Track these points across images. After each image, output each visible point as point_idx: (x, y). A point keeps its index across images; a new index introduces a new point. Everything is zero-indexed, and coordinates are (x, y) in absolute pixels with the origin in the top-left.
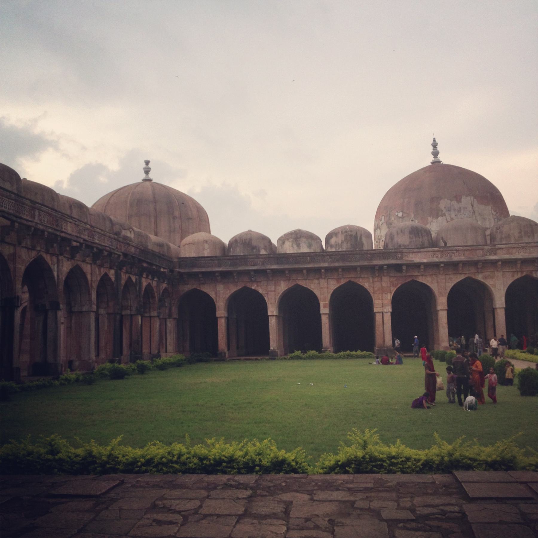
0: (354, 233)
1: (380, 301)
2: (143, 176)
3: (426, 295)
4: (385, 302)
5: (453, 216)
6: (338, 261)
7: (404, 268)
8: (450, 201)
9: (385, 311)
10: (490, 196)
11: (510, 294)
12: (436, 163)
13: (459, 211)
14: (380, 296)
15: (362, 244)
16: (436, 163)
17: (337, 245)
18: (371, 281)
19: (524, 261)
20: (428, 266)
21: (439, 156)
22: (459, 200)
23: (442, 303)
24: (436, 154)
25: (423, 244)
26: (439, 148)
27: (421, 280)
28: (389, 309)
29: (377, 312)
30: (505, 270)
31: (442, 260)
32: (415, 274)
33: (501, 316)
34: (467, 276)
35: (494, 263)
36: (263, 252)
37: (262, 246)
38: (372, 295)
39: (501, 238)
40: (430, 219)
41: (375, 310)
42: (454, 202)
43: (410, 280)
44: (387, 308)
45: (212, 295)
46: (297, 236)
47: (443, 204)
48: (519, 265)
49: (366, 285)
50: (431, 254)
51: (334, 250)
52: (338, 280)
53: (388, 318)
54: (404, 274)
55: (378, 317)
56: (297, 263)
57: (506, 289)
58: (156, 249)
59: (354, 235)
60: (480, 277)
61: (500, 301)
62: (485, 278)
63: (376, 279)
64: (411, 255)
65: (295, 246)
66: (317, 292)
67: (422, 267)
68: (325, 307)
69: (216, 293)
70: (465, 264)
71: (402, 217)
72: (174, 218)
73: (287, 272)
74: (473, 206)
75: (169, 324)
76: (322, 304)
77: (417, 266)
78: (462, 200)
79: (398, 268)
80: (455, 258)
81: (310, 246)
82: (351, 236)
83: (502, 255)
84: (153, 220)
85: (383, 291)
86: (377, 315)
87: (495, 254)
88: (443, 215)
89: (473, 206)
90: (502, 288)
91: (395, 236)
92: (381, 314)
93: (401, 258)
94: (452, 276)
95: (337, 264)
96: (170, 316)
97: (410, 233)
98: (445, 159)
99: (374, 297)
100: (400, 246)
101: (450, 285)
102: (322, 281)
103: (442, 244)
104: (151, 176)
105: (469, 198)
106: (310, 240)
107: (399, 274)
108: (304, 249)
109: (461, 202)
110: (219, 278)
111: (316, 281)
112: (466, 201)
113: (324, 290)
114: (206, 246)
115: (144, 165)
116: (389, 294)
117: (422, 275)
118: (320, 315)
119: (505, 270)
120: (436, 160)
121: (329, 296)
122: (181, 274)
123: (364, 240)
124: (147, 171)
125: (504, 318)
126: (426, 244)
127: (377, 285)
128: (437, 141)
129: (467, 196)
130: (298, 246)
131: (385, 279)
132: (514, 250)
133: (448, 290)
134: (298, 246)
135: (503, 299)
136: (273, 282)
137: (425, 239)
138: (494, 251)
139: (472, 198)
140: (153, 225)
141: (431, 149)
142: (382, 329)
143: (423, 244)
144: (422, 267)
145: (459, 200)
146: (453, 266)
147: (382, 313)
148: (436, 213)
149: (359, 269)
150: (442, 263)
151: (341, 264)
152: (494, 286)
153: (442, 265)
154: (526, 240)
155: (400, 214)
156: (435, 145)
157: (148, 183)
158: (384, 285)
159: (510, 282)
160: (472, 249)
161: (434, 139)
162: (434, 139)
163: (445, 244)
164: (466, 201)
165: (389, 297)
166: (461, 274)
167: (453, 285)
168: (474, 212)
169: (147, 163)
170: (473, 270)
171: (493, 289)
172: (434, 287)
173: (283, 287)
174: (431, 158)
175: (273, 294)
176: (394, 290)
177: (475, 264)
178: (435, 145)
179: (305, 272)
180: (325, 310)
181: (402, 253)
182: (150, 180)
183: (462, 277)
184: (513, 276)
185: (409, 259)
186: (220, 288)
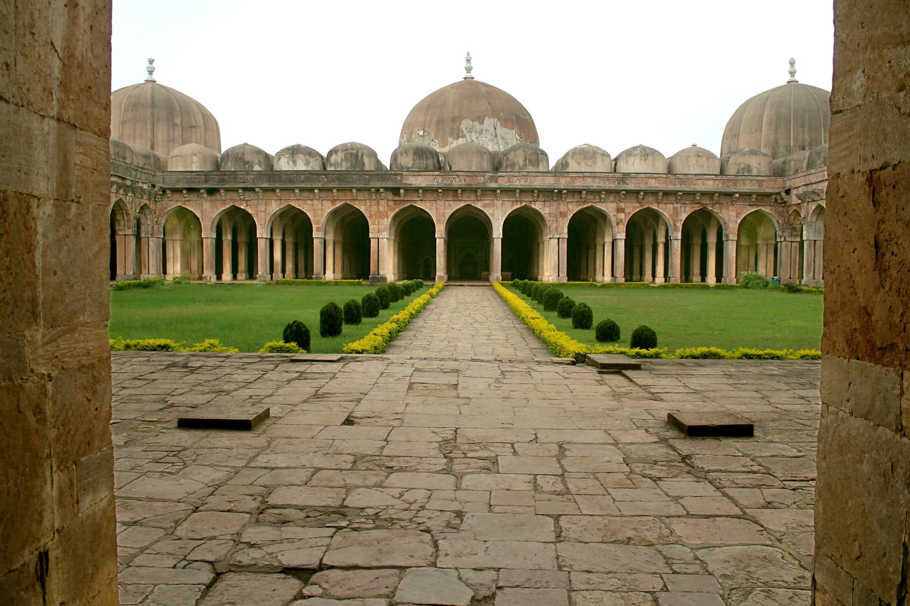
0: (355, 152)
2: (146, 76)
4: (382, 227)
5: (474, 138)
6: (333, 181)
7: (402, 191)
10: (519, 119)
11: (508, 224)
13: (481, 133)
15: (364, 164)
17: (336, 164)
19: (523, 191)
20: (426, 190)
22: (481, 122)
23: (440, 231)
25: (427, 167)
35: (494, 191)
36: (257, 168)
37: (256, 161)
39: (507, 166)
40: (450, 139)
42: (476, 124)
43: (409, 204)
46: (294, 151)
47: (465, 124)
49: (362, 209)
50: (431, 178)
51: (333, 169)
52: (334, 201)
55: (373, 243)
56: (291, 181)
58: (141, 162)
59: (356, 154)
60: (479, 205)
62: (485, 206)
63: (373, 203)
64: (411, 178)
65: (291, 163)
68: (318, 230)
69: (202, 212)
71: (423, 136)
72: (175, 125)
73: (277, 191)
75: (150, 242)
76: (314, 227)
77: (416, 190)
79: (395, 191)
80: (456, 183)
81: (307, 163)
82: (352, 154)
83: (503, 182)
84: (149, 127)
85: (381, 215)
87: (496, 182)
88: (465, 136)
91: (399, 157)
93: (401, 181)
94: (451, 203)
95: (331, 185)
96: (152, 235)
97: (414, 154)
98: (479, 76)
100: (403, 168)
101: (449, 212)
102: (316, 202)
104: (155, 77)
106: (307, 157)
107: (397, 198)
108: (301, 167)
110: (205, 195)
111: (310, 202)
112: (489, 122)
113: (319, 212)
114: (195, 159)
115: (148, 64)
120: (468, 75)
122: (164, 191)
123: (366, 160)
124: (151, 72)
126: (431, 167)
127: (374, 208)
130: (295, 162)
131: (383, 202)
132: (515, 179)
134: (295, 162)
136: (264, 202)
137: (430, 162)
140: (149, 134)
143: (427, 167)
144: (421, 191)
146: (452, 192)
148: (457, 135)
150: (440, 188)
151: (336, 185)
154: (531, 169)
155: (421, 133)
157: (150, 85)
158: (381, 208)
160: (472, 174)
163: (451, 168)
164: (489, 122)
165: (387, 222)
169: (151, 61)
170: (473, 197)
173: (275, 207)
175: (264, 212)
179: (297, 191)
181: (402, 175)
183: (462, 204)
185: (409, 182)
186: (207, 206)
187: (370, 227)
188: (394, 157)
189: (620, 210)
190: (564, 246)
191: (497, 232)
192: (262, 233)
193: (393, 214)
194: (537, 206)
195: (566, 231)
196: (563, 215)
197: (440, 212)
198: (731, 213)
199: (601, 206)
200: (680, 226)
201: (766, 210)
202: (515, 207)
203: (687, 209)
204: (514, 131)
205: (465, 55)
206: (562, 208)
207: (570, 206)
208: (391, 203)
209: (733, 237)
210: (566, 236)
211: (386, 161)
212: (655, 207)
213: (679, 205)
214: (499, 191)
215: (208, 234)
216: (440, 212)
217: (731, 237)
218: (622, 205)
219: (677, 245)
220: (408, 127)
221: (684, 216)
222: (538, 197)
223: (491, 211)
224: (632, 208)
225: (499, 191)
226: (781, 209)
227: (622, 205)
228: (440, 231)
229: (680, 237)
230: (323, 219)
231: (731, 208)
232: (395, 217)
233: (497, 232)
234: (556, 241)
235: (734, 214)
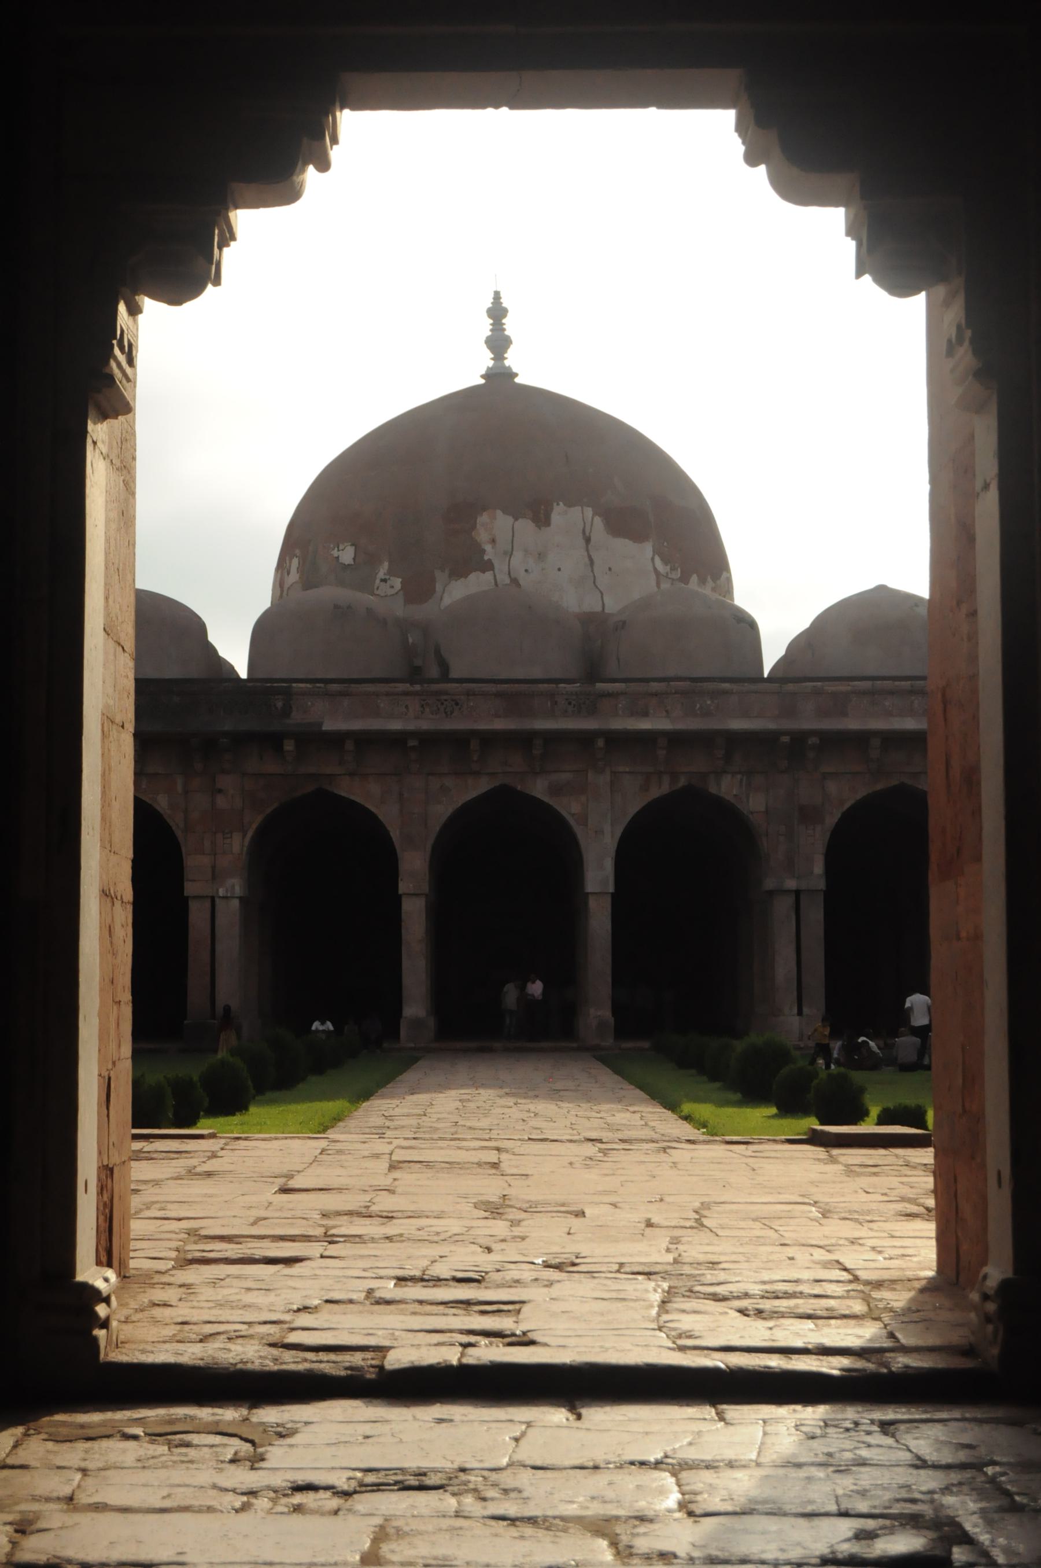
3: (368, 847)
7: (289, 746)
9: (221, 892)
12: (499, 377)
16: (499, 377)
18: (180, 788)
22: (542, 520)
24: (498, 343)
26: (510, 326)
27: (350, 790)
28: (234, 886)
29: (195, 897)
30: (621, 769)
31: (411, 726)
33: (599, 921)
34: (496, 783)
35: (584, 740)
41: (190, 889)
44: (230, 882)
48: (662, 753)
53: (230, 913)
55: (197, 915)
60: (539, 789)
62: (556, 790)
67: (349, 745)
70: (489, 740)
74: (588, 540)
78: (556, 518)
86: (193, 906)
89: (588, 540)
90: (607, 828)
92: (208, 904)
93: (286, 712)
101: (442, 811)
103: (434, 672)
109: (547, 522)
117: (352, 774)
119: (621, 769)
125: (609, 926)
128: (505, 302)
129: (570, 504)
133: (436, 827)
135: (609, 865)
138: (589, 705)
139: (589, 512)
141: (485, 326)
144: (349, 745)
145: (542, 520)
147: (213, 899)
150: (413, 734)
153: (412, 743)
155: (347, 555)
156: (497, 312)
159: (633, 809)
161: (497, 296)
162: (497, 296)
163: (444, 667)
165: (238, 844)
167: (450, 810)
172: (388, 814)
174: (485, 360)
176: (254, 821)
177: (523, 740)
178: (497, 312)
188: (264, 634)
190: (815, 915)
191: (599, 874)
194: (727, 787)
195: (819, 868)
196: (809, 815)
197: (414, 815)
202: (656, 792)
204: (648, 548)
205: (488, 303)
207: (832, 787)
210: (822, 885)
211: (235, 652)
214: (600, 743)
216: (414, 815)
223: (575, 808)
228: (414, 868)
233: (599, 874)
234: (790, 900)
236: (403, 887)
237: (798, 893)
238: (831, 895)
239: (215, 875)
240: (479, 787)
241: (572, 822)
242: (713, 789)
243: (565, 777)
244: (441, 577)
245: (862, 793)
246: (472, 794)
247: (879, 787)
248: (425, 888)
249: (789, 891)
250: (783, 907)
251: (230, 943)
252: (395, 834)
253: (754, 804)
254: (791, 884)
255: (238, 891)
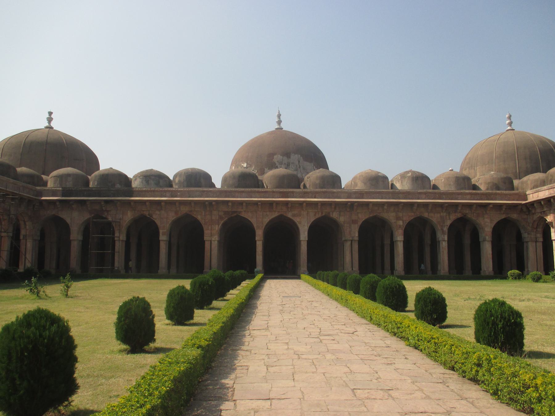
1: (209, 232)
8: (282, 157)
14: (210, 228)
19: (323, 204)
21: (281, 124)
24: (279, 122)
27: (243, 215)
32: (239, 210)
34: (280, 214)
38: (203, 225)
40: (266, 170)
41: (205, 238)
42: (285, 158)
43: (235, 214)
45: (68, 221)
49: (199, 218)
53: (215, 244)
54: (230, 210)
57: (309, 225)
60: (289, 215)
61: (304, 236)
62: (294, 215)
66: (158, 222)
68: (163, 234)
74: (299, 162)
76: (161, 231)
78: (292, 157)
89: (299, 162)
90: (306, 224)
94: (268, 213)
98: (287, 127)
99: (205, 227)
101: (266, 220)
105: (296, 155)
109: (290, 158)
111: (158, 212)
116: (217, 226)
118: (159, 242)
121: (168, 225)
135: (306, 233)
139: (299, 156)
142: (209, 254)
149: (193, 204)
152: (300, 223)
158: (214, 218)
159: (312, 220)
165: (217, 228)
166: (275, 211)
168: (300, 167)
169: (50, 113)
171: (299, 226)
172: (254, 221)
180: (163, 237)
182: (52, 128)
184: (315, 215)
186: (75, 214)
187: (207, 232)
189: (398, 218)
190: (356, 246)
192: (120, 236)
193: (222, 222)
194: (335, 215)
195: (357, 235)
196: (354, 222)
198: (486, 220)
199: (385, 215)
200: (446, 229)
201: (514, 216)
203: (451, 217)
206: (354, 217)
208: (222, 214)
209: (489, 238)
212: (426, 215)
213: (445, 214)
214: (305, 204)
215: (76, 236)
217: (487, 238)
218: (400, 214)
219: (444, 246)
220: (236, 162)
221: (449, 223)
222: (335, 208)
223: (298, 220)
224: (408, 216)
225: (305, 204)
226: (525, 217)
227: (400, 214)
229: (446, 238)
230: (168, 226)
231: (486, 216)
232: (224, 225)
234: (349, 243)
235: (487, 220)
236: (257, 238)
237: (352, 241)
238: (360, 242)
239: (212, 235)
240: (275, 215)
241: (297, 223)
242: (331, 216)
243: (296, 212)
244: (266, 170)
245: (367, 217)
246: (274, 216)
247: (371, 215)
248: (262, 239)
249: (350, 240)
250: (347, 245)
251: (215, 251)
252: (255, 226)
253: (341, 219)
254: (351, 239)
255: (217, 239)
